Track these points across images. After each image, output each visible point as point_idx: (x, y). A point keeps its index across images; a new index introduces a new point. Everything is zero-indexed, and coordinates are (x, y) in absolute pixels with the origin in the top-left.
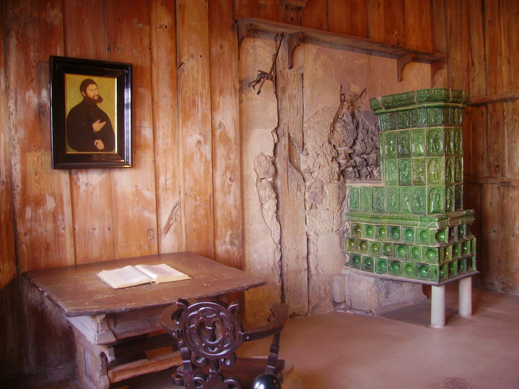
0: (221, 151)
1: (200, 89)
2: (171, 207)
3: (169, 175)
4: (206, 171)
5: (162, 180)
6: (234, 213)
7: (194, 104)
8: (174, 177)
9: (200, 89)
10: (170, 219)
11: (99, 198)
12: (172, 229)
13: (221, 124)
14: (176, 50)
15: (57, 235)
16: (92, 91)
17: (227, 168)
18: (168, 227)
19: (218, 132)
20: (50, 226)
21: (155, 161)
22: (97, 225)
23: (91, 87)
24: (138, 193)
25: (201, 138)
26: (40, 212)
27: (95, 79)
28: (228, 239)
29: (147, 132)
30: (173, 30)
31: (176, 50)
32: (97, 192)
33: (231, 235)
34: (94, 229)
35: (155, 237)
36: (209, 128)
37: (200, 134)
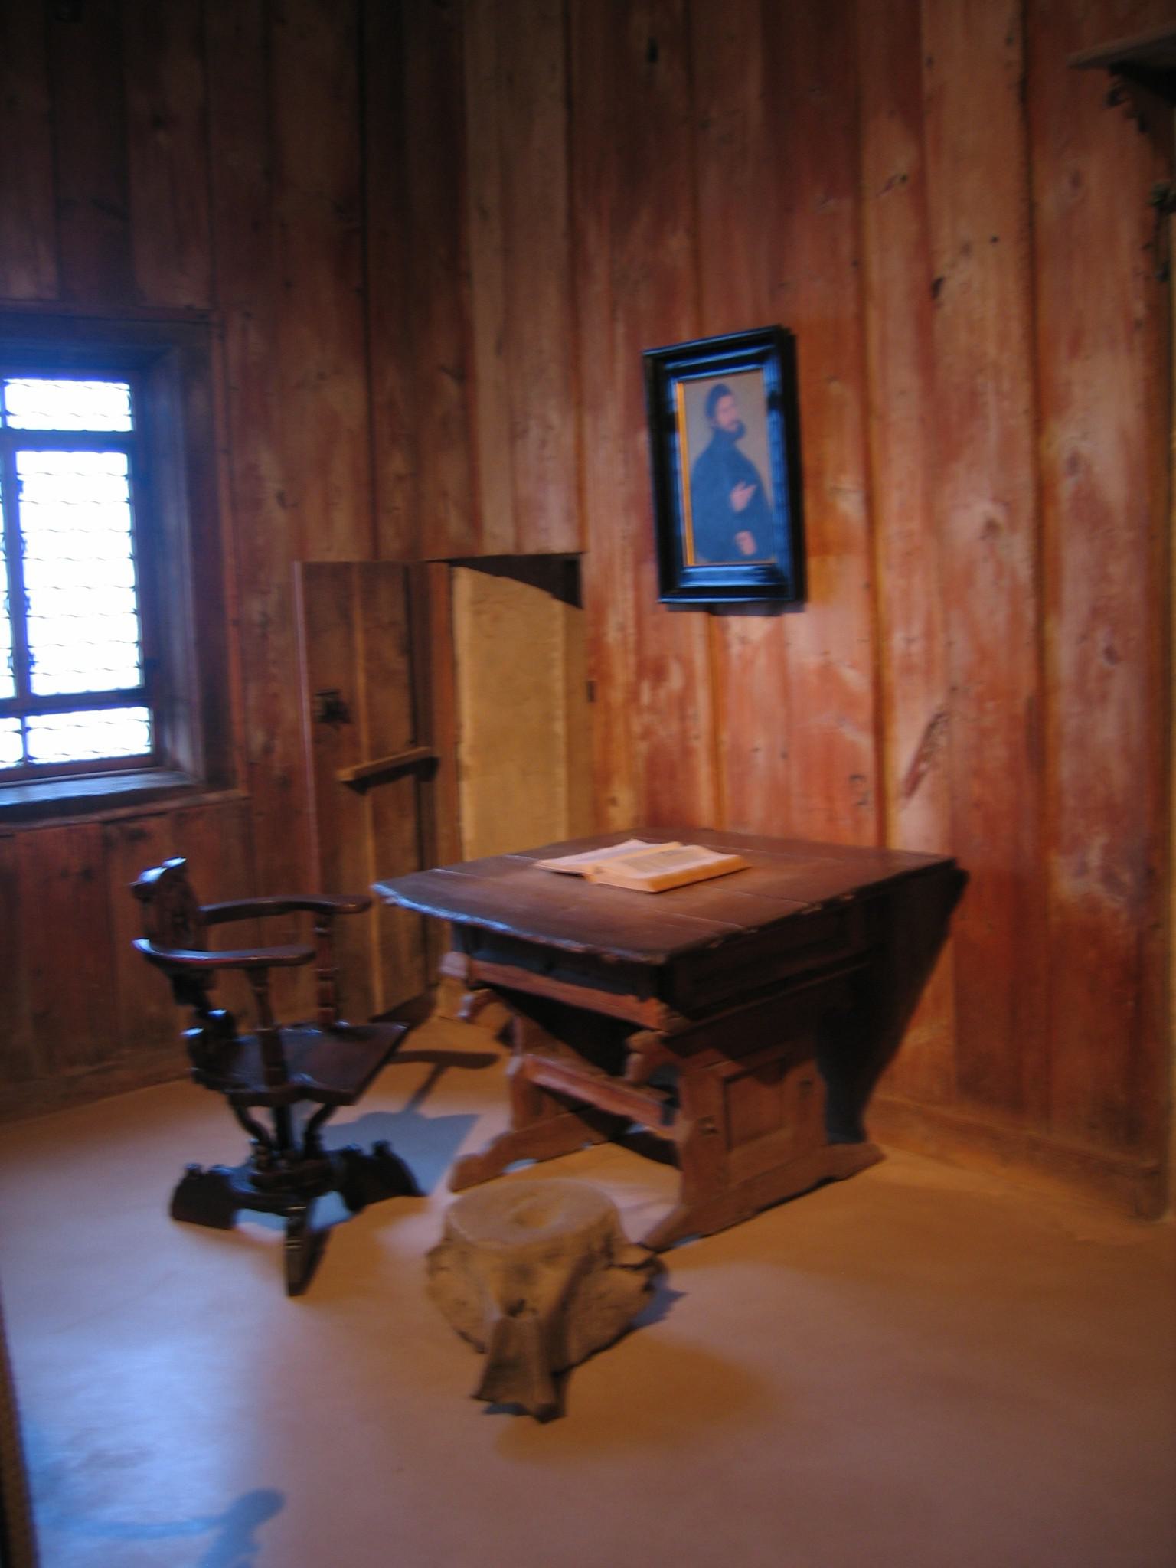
0: (1075, 554)
1: (991, 350)
2: (922, 720)
3: (917, 629)
4: (1015, 618)
5: (897, 641)
6: (1120, 774)
7: (973, 404)
8: (929, 634)
9: (991, 350)
10: (921, 757)
11: (761, 681)
12: (925, 785)
13: (1074, 462)
14: (924, 248)
15: (687, 752)
16: (727, 413)
17: (1097, 613)
18: (914, 781)
19: (1066, 488)
20: (674, 727)
21: (872, 589)
22: (760, 741)
23: (725, 402)
24: (827, 672)
25: (998, 514)
26: (662, 693)
27: (729, 382)
28: (1094, 857)
29: (849, 505)
30: (918, 185)
31: (924, 248)
32: (762, 661)
33: (1108, 850)
34: (756, 750)
35: (871, 798)
36: (1024, 476)
37: (995, 499)
